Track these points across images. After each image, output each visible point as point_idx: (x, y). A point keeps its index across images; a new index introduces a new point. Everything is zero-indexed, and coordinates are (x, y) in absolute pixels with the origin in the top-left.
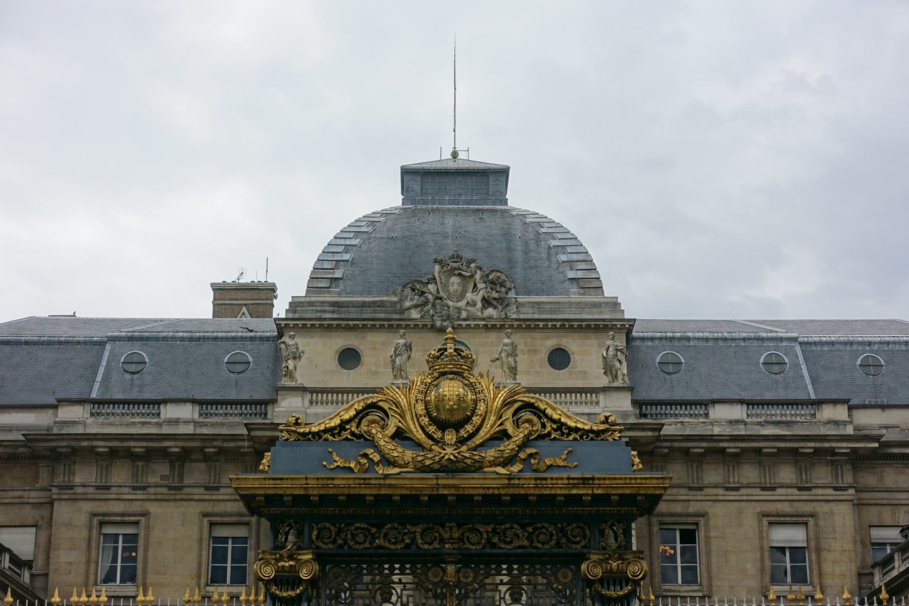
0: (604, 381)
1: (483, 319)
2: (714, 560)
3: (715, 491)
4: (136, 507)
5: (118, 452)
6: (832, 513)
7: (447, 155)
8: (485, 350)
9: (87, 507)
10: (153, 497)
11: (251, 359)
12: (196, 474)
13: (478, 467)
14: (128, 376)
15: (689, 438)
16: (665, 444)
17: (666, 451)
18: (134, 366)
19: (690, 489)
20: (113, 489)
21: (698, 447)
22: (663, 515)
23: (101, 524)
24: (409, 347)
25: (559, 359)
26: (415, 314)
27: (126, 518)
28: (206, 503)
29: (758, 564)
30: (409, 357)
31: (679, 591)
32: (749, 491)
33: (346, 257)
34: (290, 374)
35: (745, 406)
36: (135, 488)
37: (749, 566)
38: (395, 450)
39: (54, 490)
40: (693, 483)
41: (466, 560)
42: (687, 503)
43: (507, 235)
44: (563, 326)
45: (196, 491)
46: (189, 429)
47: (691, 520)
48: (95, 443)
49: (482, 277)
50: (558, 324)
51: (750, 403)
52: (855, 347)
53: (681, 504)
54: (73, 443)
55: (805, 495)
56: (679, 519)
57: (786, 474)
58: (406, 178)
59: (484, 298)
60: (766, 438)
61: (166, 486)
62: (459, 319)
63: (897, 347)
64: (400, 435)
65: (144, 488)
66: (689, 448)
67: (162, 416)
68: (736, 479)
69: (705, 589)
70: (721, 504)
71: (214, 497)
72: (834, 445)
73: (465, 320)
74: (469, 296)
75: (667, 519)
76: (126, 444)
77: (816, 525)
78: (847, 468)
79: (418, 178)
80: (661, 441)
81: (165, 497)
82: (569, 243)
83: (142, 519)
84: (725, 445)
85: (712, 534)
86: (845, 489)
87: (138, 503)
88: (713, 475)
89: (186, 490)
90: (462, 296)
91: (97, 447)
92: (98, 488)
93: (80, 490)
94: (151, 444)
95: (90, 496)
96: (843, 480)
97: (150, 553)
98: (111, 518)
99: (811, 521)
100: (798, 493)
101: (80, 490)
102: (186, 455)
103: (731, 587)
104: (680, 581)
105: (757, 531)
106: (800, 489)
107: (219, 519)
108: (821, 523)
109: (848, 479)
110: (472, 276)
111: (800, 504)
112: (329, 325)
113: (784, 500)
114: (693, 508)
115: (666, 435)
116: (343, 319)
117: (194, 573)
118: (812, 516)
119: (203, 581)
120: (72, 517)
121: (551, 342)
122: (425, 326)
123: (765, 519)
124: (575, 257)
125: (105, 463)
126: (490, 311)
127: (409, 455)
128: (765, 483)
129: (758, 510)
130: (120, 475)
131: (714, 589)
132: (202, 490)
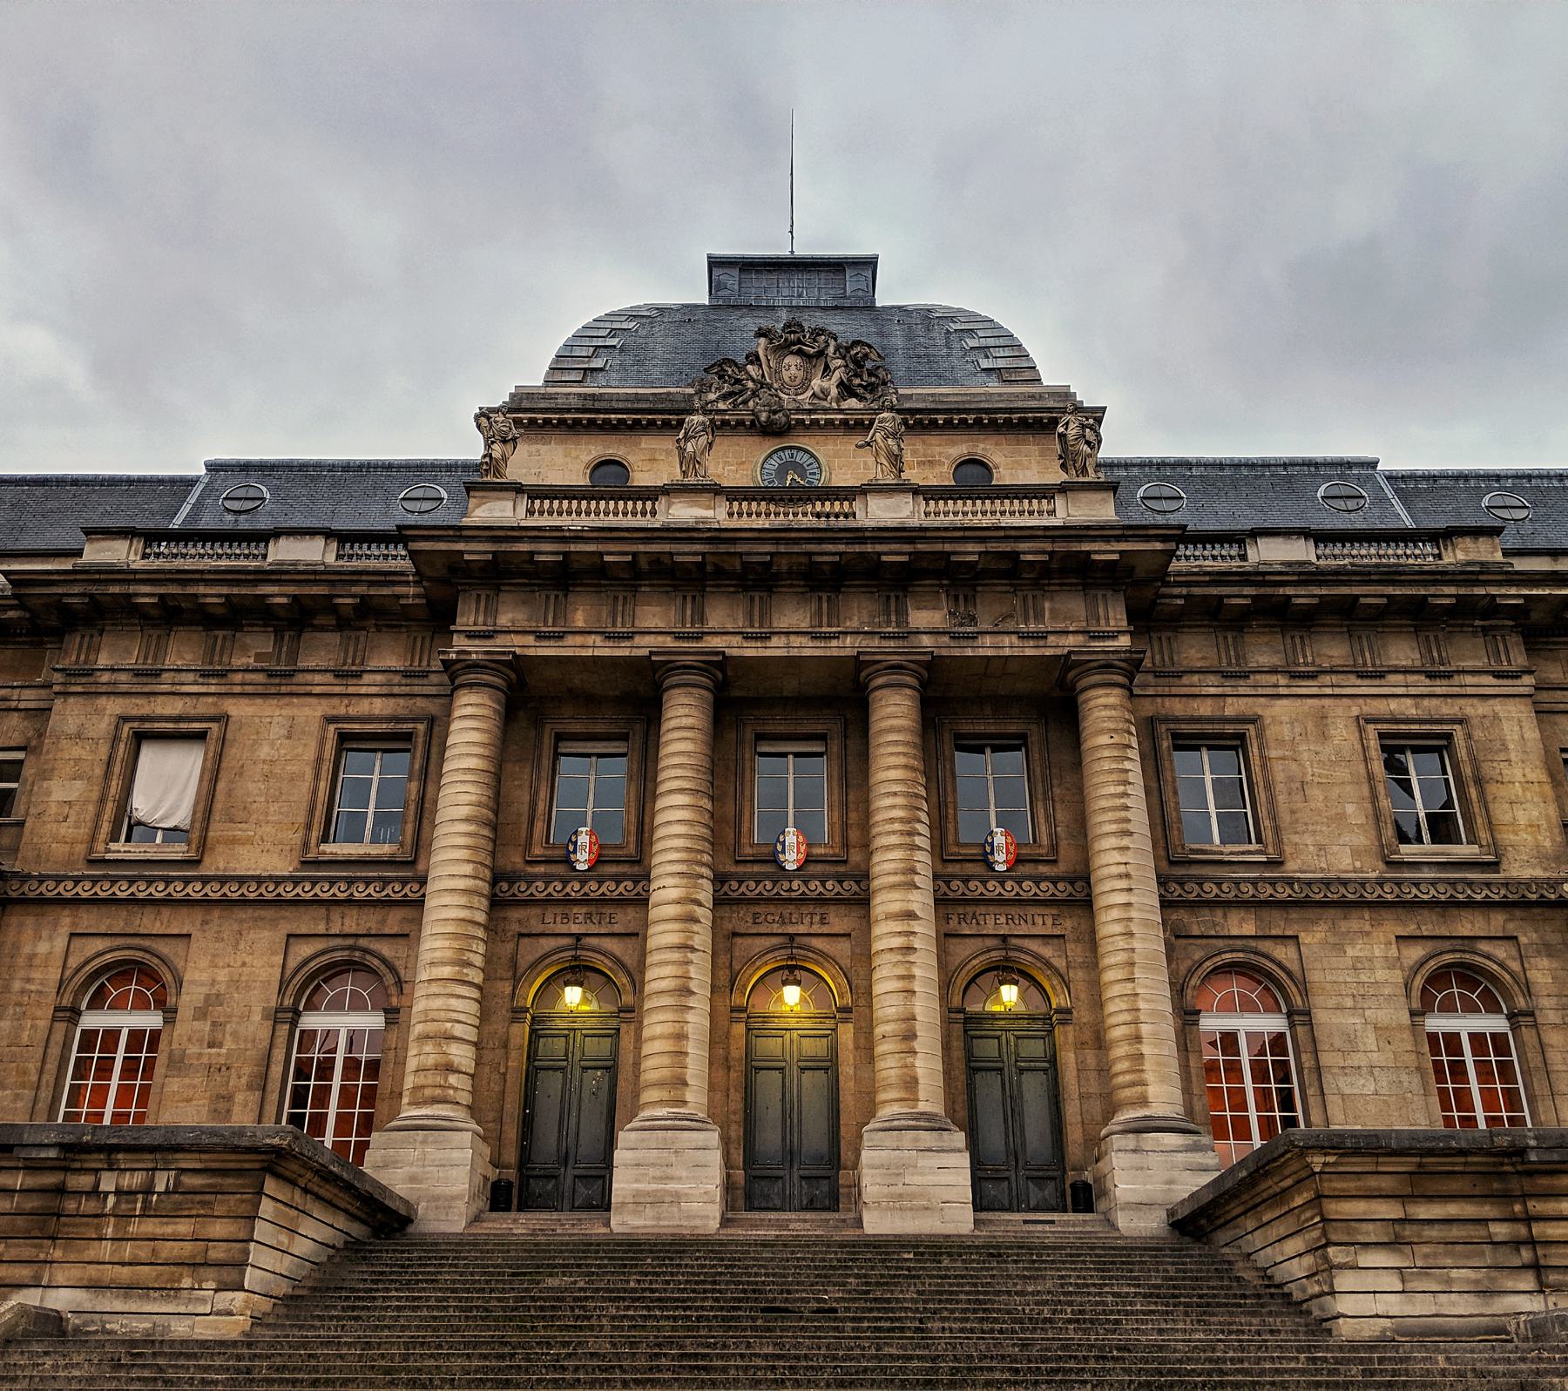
1: (841, 411)
2: (1281, 798)
3: (1273, 679)
4: (204, 707)
6: (1496, 717)
9: (114, 707)
10: (237, 689)
11: (444, 494)
12: (320, 653)
14: (230, 517)
16: (1176, 591)
17: (1180, 602)
19: (1227, 675)
20: (165, 675)
21: (1240, 596)
22: (1177, 720)
23: (140, 738)
26: (721, 406)
27: (183, 726)
28: (336, 701)
29: (1368, 806)
30: (710, 444)
31: (1221, 853)
32: (1335, 679)
33: (614, 342)
35: (1311, 543)
36: (205, 674)
37: (1350, 809)
39: (58, 677)
40: (1229, 664)
42: (1220, 700)
44: (978, 422)
45: (318, 678)
47: (1230, 729)
48: (132, 589)
49: (837, 349)
50: (971, 418)
51: (1321, 537)
52: (1472, 483)
53: (1209, 701)
54: (93, 589)
56: (1209, 728)
57: (1402, 652)
58: (716, 272)
59: (841, 384)
61: (262, 670)
62: (799, 411)
63: (1546, 483)
65: (222, 674)
66: (1221, 597)
67: (269, 559)
68: (1310, 659)
69: (1271, 850)
70: (1285, 702)
71: (351, 690)
72: (1493, 591)
73: (810, 412)
74: (817, 383)
75: (1186, 728)
76: (190, 590)
77: (1469, 736)
78: (1515, 641)
79: (736, 272)
80: (1168, 584)
81: (260, 689)
82: (980, 326)
83: (214, 726)
84: (1289, 591)
85: (1273, 753)
86: (1515, 675)
87: (210, 700)
89: (299, 678)
90: (805, 384)
91: (136, 595)
92: (137, 673)
93: (105, 677)
94: (235, 591)
95: (124, 688)
96: (1509, 661)
97: (221, 785)
98: (156, 725)
99: (1458, 732)
100: (1428, 682)
101: (105, 677)
103: (1321, 847)
104: (1217, 839)
105: (1358, 747)
106: (1431, 675)
107: (356, 727)
108: (1478, 734)
109: (1519, 659)
110: (821, 353)
111: (1435, 702)
112: (577, 422)
114: (1232, 708)
115: (1179, 574)
116: (598, 411)
117: (301, 819)
118: (1460, 722)
119: (315, 834)
120: (83, 726)
122: (740, 423)
123: (1371, 727)
124: (991, 342)
125: (155, 632)
126: (853, 403)
128: (1365, 664)
129: (1355, 711)
130: (182, 652)
131: (1288, 849)
132: (329, 678)
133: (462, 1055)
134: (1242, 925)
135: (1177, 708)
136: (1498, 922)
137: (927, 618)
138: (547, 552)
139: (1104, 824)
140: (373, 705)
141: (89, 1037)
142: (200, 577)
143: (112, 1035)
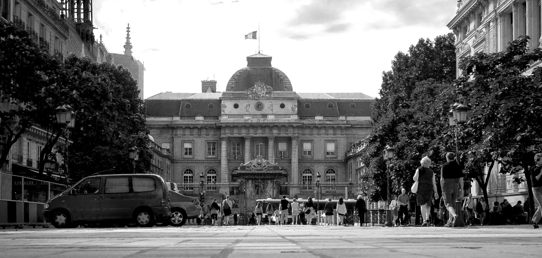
0: (291, 112)
5: (188, 127)
7: (257, 53)
8: (266, 104)
12: (204, 132)
13: (262, 170)
15: (310, 124)
18: (188, 106)
24: (249, 105)
25: (282, 106)
34: (224, 111)
38: (253, 168)
41: (261, 179)
43: (271, 75)
46: (202, 123)
55: (335, 136)
57: (331, 132)
60: (327, 124)
64: (254, 166)
88: (315, 131)
102: (202, 128)
113: (330, 137)
121: (281, 102)
126: (267, 95)
127: (255, 168)
130: (187, 132)
133: (227, 181)
134: (308, 165)
135: (304, 139)
136: (336, 164)
137: (275, 132)
138: (232, 125)
139: (293, 156)
140: (211, 138)
141: (185, 177)
142: (190, 124)
143: (187, 177)
